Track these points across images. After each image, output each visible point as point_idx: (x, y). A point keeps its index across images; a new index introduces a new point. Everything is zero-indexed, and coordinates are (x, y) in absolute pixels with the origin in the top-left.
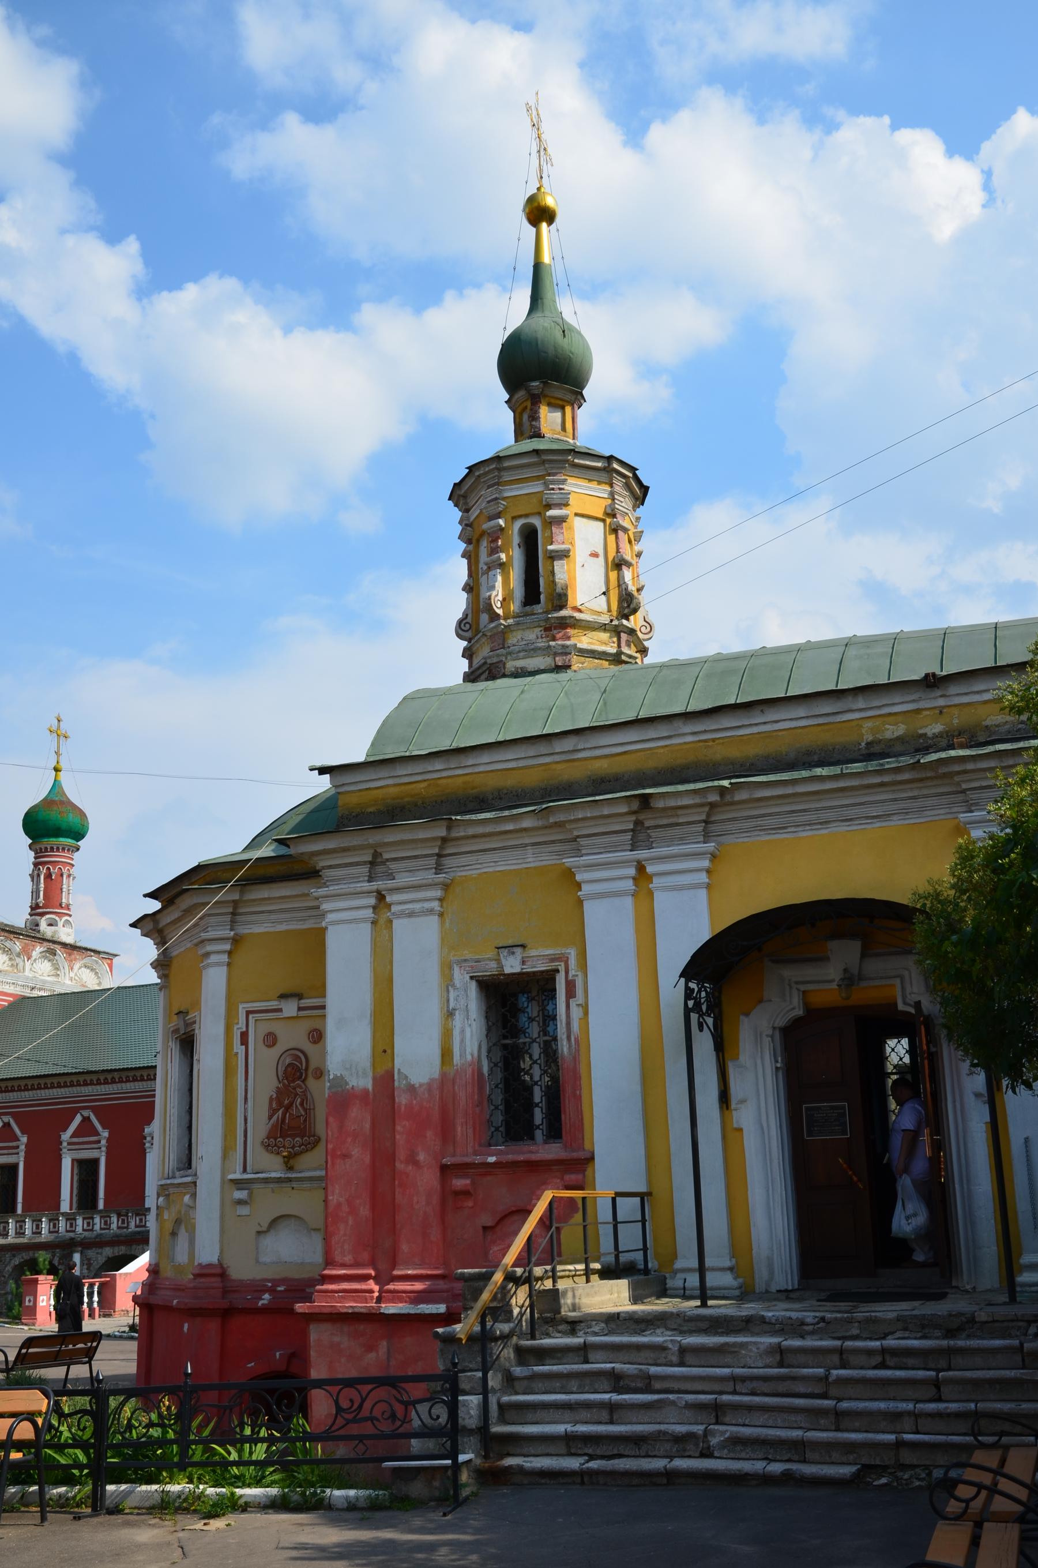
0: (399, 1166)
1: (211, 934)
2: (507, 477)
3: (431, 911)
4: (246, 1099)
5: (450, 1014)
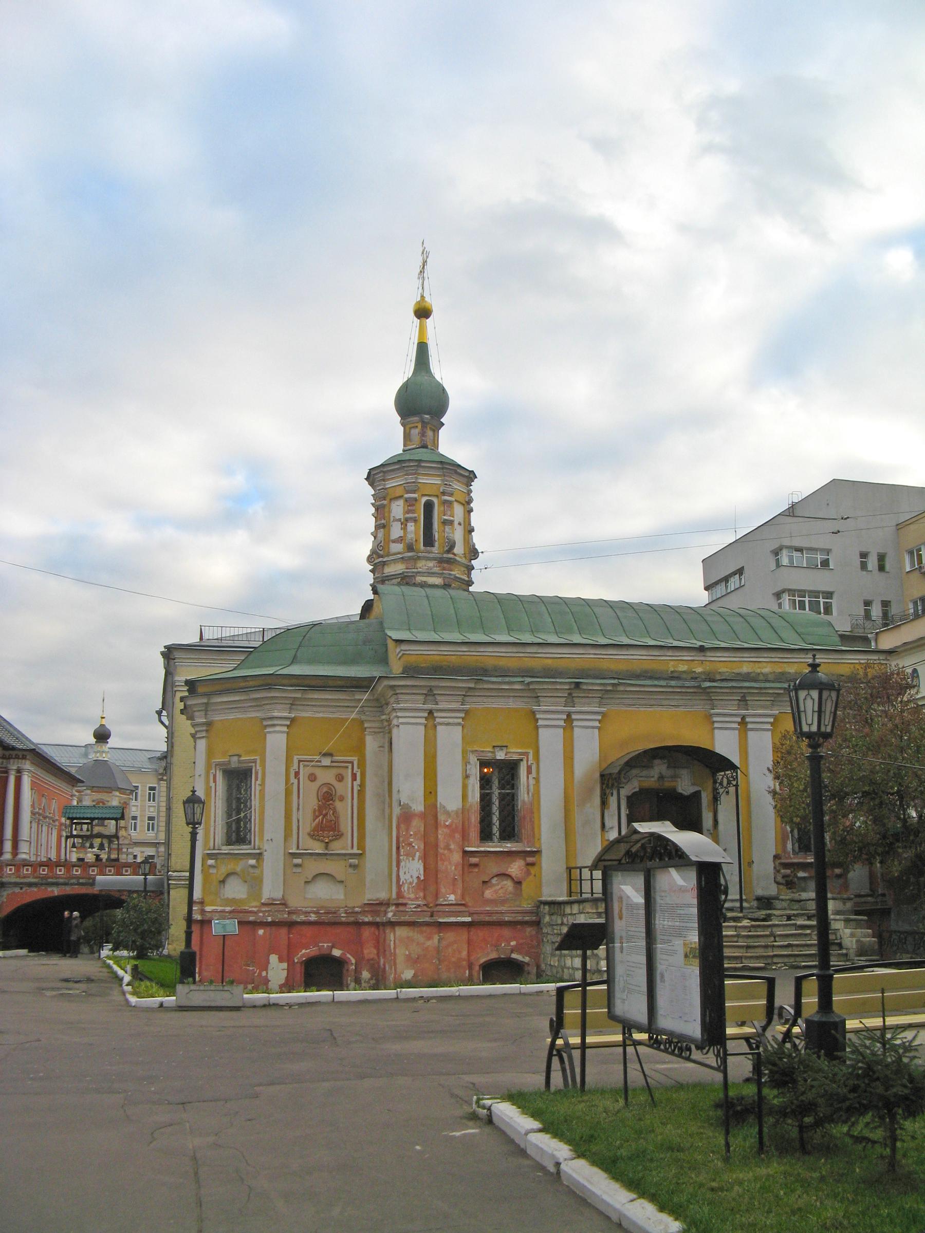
0: (441, 851)
1: (276, 714)
2: (421, 471)
3: (459, 724)
4: (298, 809)
5: (467, 777)
